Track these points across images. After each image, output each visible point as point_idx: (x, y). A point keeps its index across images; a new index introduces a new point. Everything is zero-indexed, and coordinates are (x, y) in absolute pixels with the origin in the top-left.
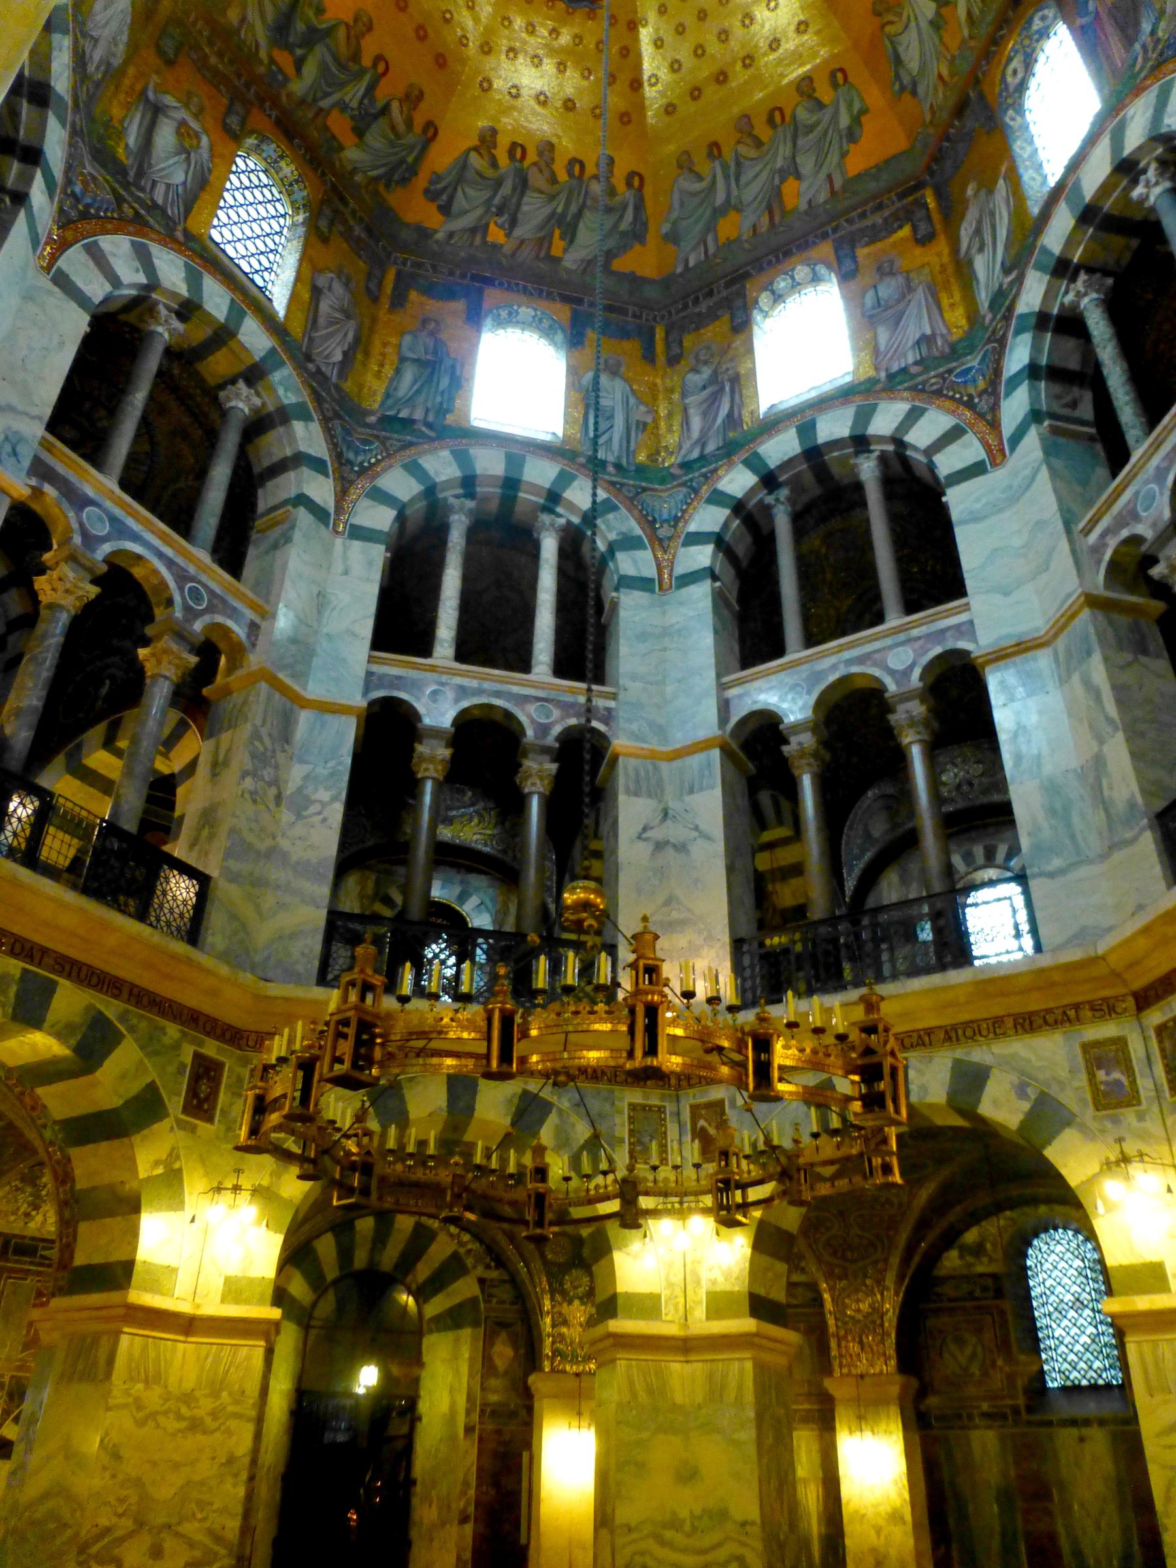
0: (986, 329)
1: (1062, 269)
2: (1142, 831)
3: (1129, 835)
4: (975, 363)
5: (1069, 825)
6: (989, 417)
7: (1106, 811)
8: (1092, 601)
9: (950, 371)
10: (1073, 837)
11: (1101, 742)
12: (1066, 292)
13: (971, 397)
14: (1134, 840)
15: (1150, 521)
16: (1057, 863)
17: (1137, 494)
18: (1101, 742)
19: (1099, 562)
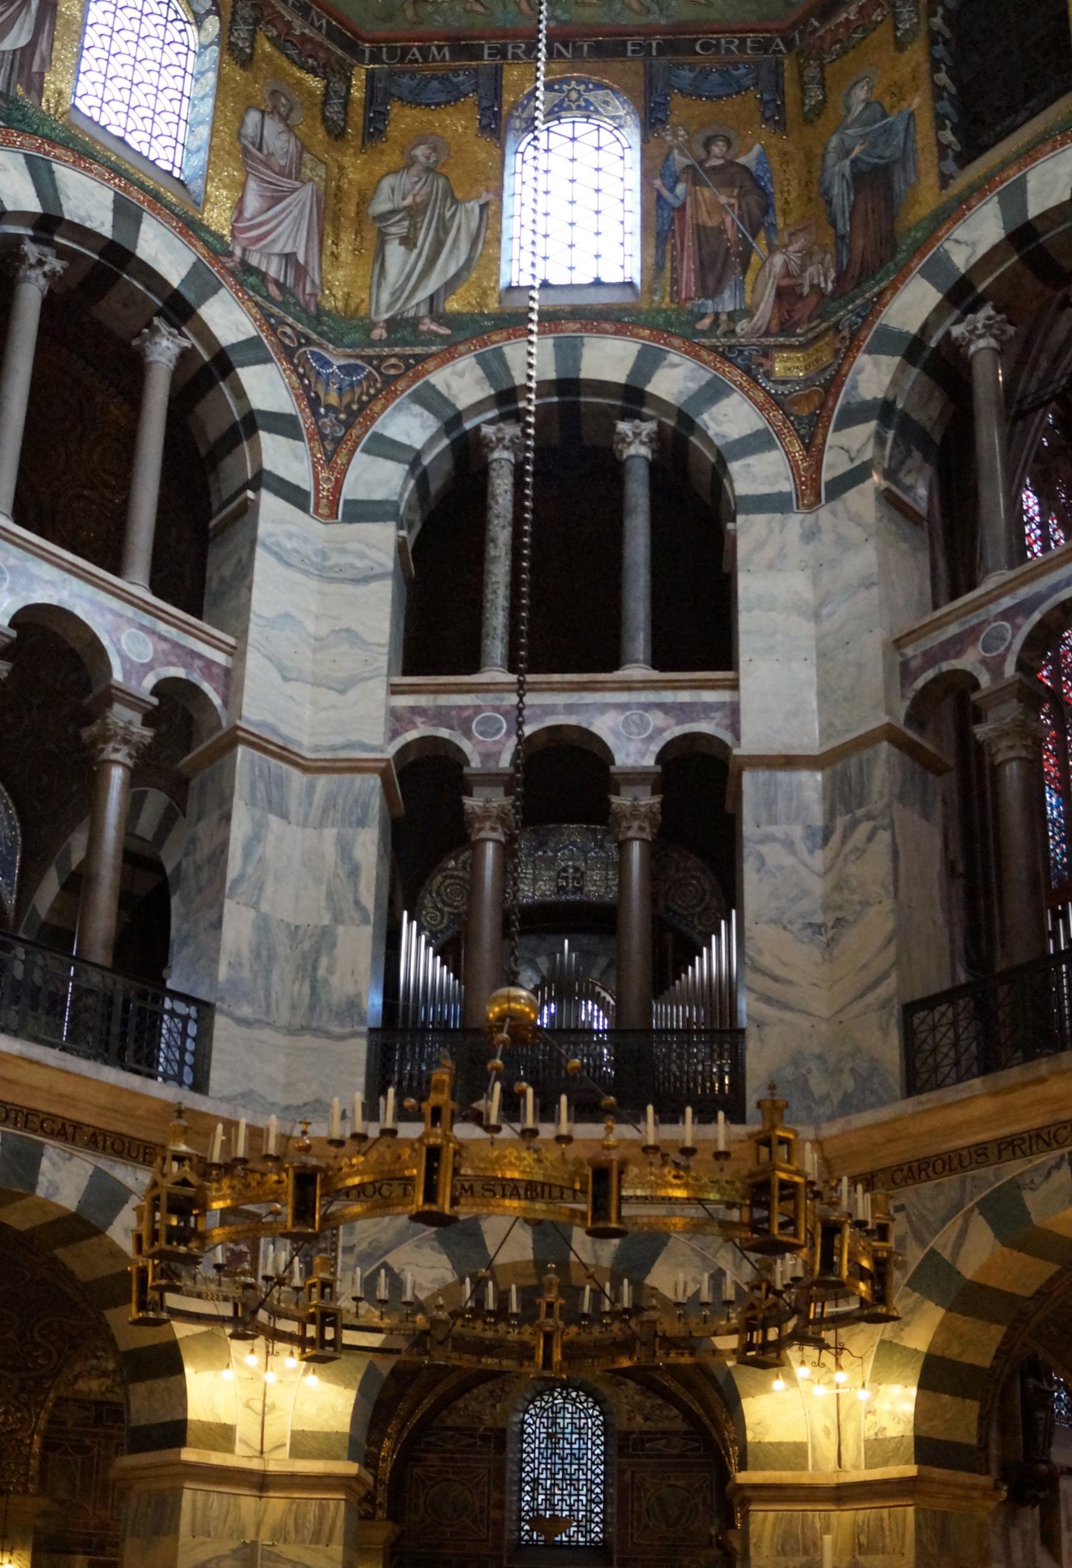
0: (372, 344)
1: (506, 398)
2: (355, 1035)
3: (335, 1029)
4: (337, 362)
5: (268, 978)
6: (329, 448)
7: (313, 991)
8: (384, 774)
9: (309, 342)
10: (268, 991)
11: (337, 920)
12: (490, 422)
13: (318, 396)
14: (342, 1038)
15: (481, 749)
16: (246, 1011)
17: (478, 709)
18: (337, 920)
19: (394, 734)
